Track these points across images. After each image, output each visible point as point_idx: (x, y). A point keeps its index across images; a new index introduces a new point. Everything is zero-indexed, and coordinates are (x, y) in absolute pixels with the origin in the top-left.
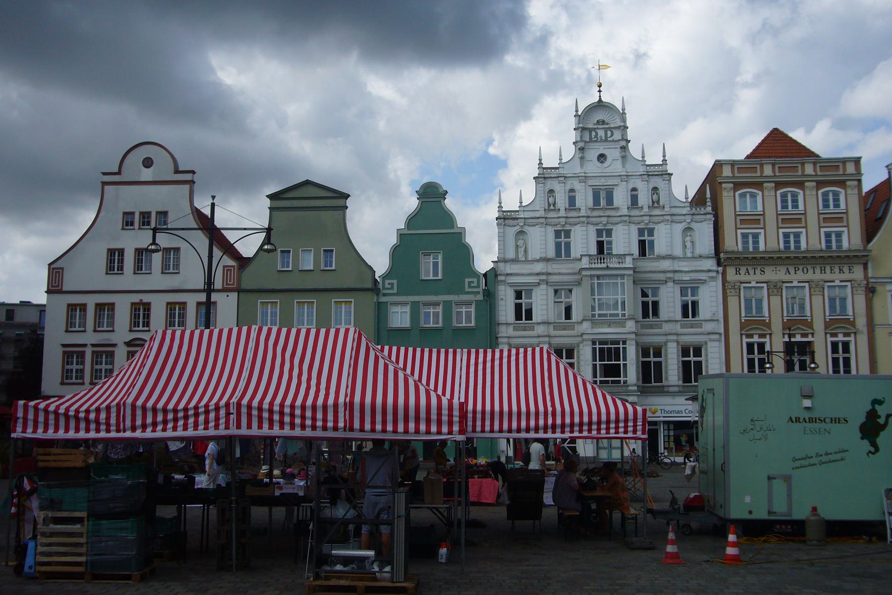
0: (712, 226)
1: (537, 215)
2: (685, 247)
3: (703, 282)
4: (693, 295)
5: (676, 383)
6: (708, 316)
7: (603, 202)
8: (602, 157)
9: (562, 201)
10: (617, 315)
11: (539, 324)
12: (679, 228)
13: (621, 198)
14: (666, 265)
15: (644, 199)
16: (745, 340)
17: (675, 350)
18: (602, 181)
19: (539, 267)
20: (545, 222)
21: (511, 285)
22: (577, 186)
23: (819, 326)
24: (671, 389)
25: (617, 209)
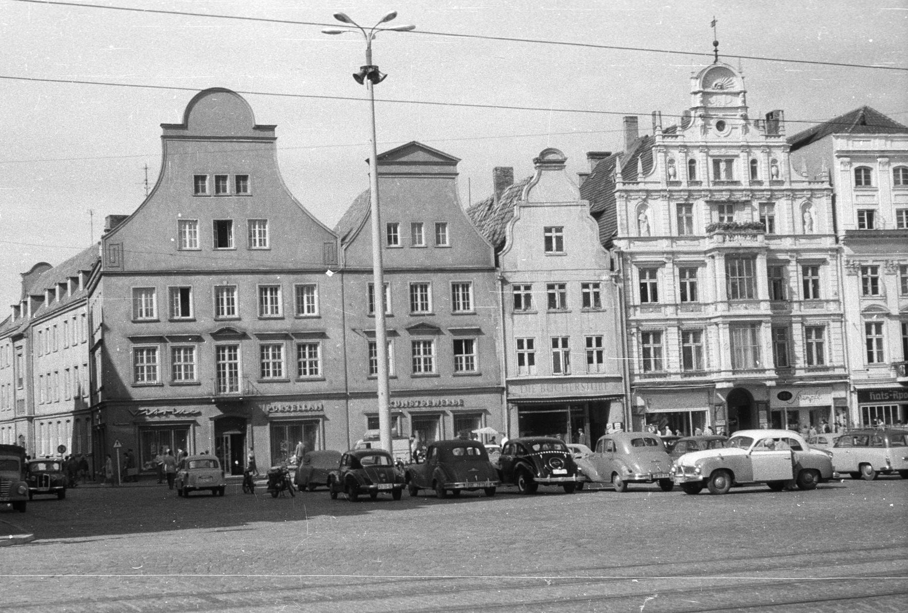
0: (830, 201)
1: (660, 187)
2: (804, 223)
3: (824, 261)
4: (691, 277)
5: (803, 365)
6: (831, 297)
7: (723, 177)
9: (682, 174)
11: (666, 305)
12: (798, 203)
13: (740, 170)
14: (787, 244)
15: (762, 175)
17: (800, 332)
18: (723, 152)
19: (664, 245)
20: (669, 196)
21: (637, 264)
22: (698, 156)
25: (736, 183)
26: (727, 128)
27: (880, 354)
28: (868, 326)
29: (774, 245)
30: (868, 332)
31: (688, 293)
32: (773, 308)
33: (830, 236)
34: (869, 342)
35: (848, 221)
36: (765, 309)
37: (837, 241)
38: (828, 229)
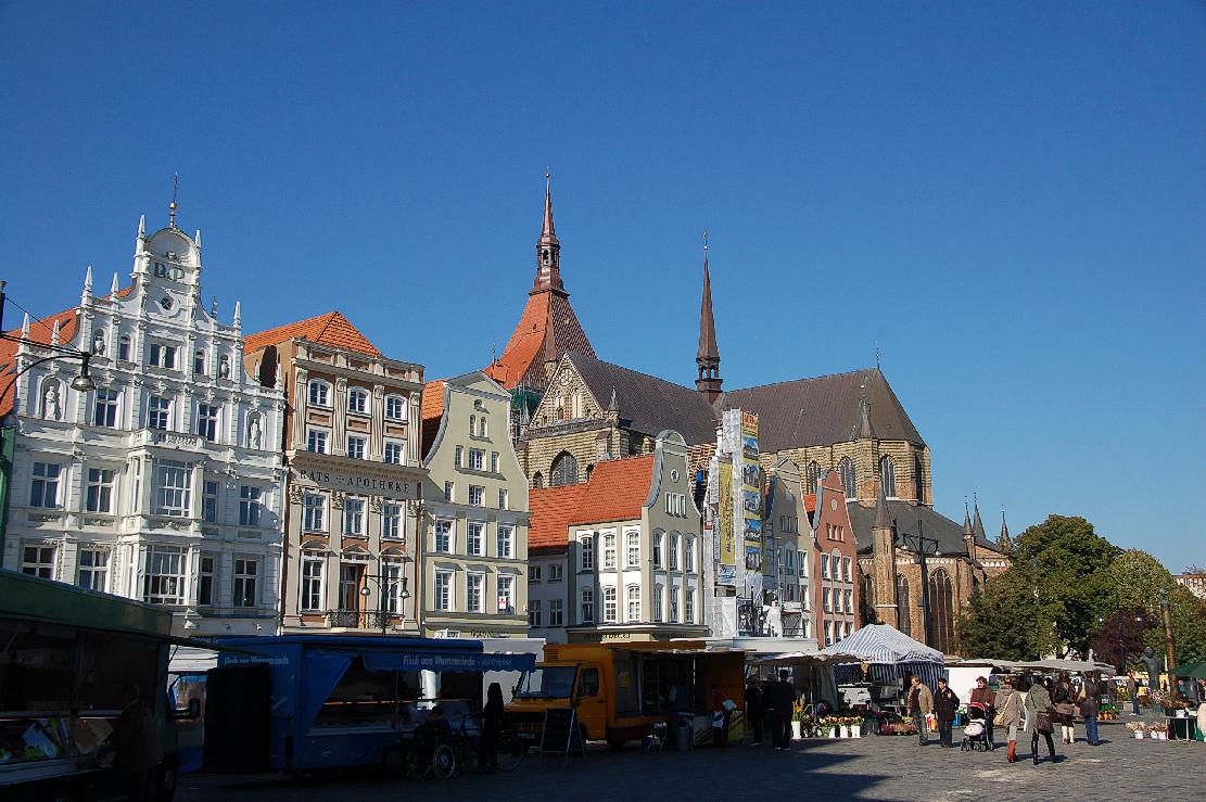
8: (167, 303)
10: (179, 513)
13: (183, 361)
16: (304, 557)
18: (164, 334)
22: (137, 337)
23: (373, 548)
24: (223, 612)
26: (174, 308)
27: (316, 599)
28: (307, 564)
29: (214, 456)
30: (306, 572)
31: (95, 499)
32: (204, 531)
33: (278, 454)
34: (306, 582)
35: (298, 443)
36: (192, 531)
37: (285, 461)
38: (275, 446)
